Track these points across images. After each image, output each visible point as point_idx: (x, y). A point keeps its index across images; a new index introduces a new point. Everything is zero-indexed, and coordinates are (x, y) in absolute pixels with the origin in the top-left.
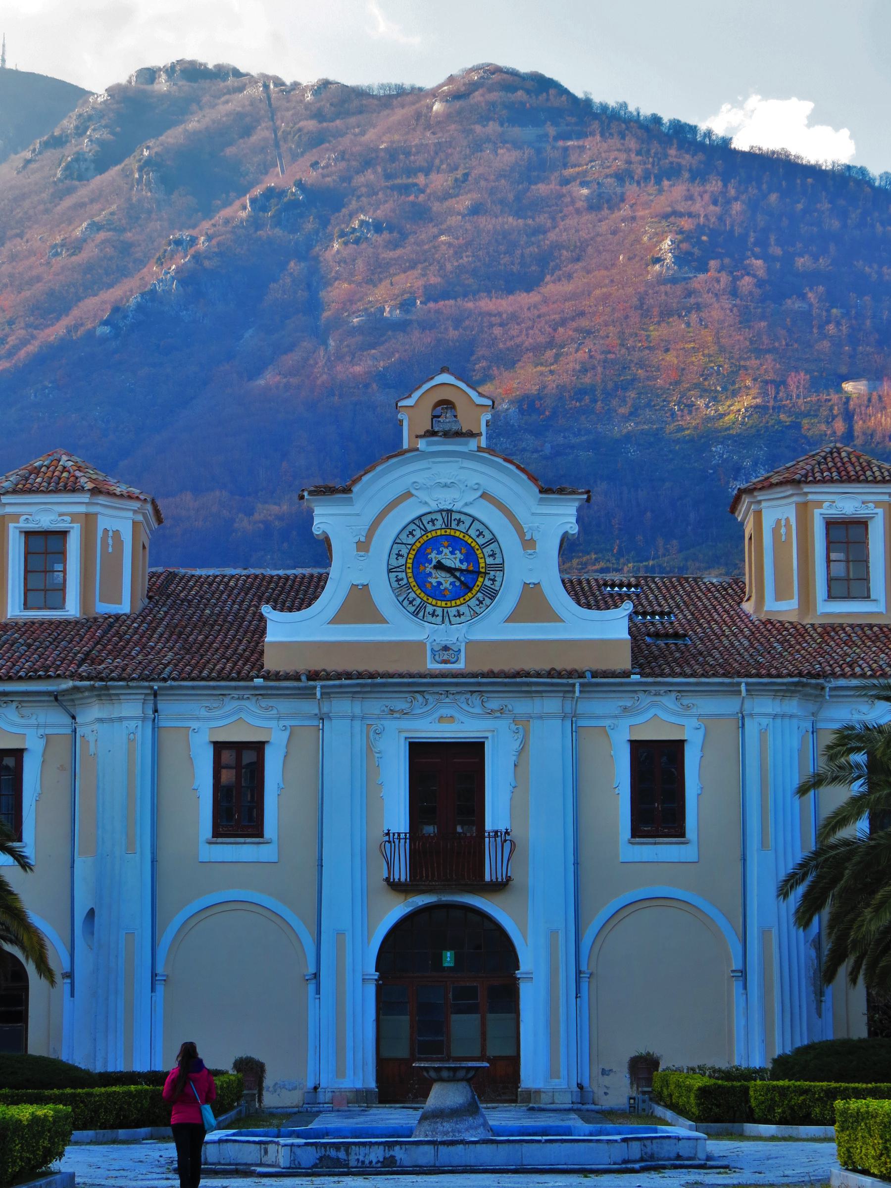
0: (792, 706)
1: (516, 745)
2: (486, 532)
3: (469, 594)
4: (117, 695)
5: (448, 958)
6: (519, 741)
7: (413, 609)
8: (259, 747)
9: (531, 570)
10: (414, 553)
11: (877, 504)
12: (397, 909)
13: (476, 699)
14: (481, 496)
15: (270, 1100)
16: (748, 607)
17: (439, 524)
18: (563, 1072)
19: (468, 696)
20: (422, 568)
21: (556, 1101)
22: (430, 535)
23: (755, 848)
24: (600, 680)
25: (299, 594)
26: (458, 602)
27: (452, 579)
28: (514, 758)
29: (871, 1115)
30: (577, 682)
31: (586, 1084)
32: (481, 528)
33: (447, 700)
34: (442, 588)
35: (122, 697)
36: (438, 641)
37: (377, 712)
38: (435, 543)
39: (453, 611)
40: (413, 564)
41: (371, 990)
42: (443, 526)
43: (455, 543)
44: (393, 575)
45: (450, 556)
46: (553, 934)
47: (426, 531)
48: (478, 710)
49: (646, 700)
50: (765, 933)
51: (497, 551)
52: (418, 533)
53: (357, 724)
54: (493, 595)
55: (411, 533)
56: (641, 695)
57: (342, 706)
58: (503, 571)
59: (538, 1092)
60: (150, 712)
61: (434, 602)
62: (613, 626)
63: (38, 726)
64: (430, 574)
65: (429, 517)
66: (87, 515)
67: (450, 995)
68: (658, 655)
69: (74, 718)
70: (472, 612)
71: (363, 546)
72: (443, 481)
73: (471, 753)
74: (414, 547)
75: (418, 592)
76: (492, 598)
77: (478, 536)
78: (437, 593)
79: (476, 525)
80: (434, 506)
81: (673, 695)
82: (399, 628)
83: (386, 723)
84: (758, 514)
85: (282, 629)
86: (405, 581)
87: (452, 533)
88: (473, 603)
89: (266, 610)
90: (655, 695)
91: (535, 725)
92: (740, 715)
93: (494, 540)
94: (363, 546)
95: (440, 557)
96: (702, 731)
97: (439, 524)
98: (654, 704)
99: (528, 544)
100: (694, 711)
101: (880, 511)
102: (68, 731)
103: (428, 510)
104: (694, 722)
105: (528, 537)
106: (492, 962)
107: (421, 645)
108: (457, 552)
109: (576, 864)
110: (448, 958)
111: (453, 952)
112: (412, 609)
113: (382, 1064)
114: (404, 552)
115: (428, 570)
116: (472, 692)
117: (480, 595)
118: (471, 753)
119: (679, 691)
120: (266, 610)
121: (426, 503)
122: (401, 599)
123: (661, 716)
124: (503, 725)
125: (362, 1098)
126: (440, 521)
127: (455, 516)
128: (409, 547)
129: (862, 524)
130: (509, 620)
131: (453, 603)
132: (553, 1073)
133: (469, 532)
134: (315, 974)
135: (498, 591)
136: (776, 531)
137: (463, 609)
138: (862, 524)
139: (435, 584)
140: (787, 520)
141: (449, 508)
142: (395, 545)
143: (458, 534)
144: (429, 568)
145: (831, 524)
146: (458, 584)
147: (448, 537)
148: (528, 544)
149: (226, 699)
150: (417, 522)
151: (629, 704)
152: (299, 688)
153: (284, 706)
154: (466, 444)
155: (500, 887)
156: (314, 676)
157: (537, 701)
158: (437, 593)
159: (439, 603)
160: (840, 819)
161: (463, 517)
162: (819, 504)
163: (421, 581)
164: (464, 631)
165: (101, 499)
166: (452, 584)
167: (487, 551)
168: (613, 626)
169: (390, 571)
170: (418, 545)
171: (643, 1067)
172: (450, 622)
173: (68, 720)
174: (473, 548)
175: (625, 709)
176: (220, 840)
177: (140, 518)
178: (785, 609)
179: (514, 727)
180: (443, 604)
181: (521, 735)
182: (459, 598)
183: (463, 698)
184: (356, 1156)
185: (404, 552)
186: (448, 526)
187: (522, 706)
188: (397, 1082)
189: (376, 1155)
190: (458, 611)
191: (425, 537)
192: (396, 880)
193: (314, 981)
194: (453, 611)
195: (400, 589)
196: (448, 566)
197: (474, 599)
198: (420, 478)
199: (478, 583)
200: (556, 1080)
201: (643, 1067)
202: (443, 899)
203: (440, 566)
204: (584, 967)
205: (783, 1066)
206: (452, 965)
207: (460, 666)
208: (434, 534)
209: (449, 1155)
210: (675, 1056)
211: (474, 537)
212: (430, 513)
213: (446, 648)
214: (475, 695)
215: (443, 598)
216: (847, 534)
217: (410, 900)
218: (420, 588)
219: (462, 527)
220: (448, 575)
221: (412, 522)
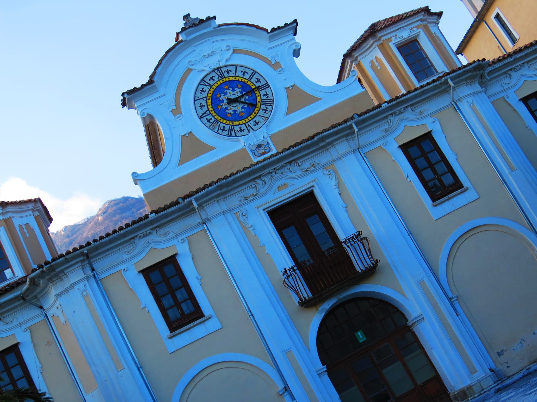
1: (334, 182)
2: (247, 70)
3: (256, 109)
4: (62, 271)
5: (360, 336)
6: (334, 179)
7: (227, 133)
8: (172, 260)
9: (285, 79)
10: (210, 101)
11: (417, 27)
12: (314, 319)
13: (294, 167)
14: (233, 53)
17: (216, 78)
18: (477, 367)
19: (289, 166)
20: (219, 107)
21: (484, 387)
23: (508, 173)
26: (252, 116)
27: (241, 106)
28: (337, 190)
30: (352, 122)
31: (493, 367)
32: (244, 69)
33: (277, 175)
34: (238, 113)
35: (66, 271)
36: (252, 144)
37: (237, 203)
38: (220, 89)
39: (252, 123)
40: (212, 107)
41: (326, 378)
42: (220, 78)
43: (232, 84)
44: (204, 119)
46: (421, 283)
47: (211, 86)
48: (299, 173)
49: (395, 120)
51: (260, 77)
52: (206, 89)
53: (229, 215)
55: (202, 91)
56: (391, 118)
57: (213, 209)
58: (269, 87)
59: (470, 388)
60: (90, 273)
61: (237, 123)
63: (20, 324)
64: (226, 109)
65: (208, 77)
66: (5, 221)
67: (375, 359)
69: (41, 307)
70: (264, 118)
71: (177, 111)
72: (206, 53)
74: (208, 98)
76: (272, 105)
77: (244, 75)
78: (236, 117)
80: (208, 70)
81: (409, 109)
82: (224, 149)
83: (246, 207)
84: (359, 66)
86: (213, 120)
87: (227, 79)
88: (261, 113)
90: (399, 114)
91: (338, 165)
92: (453, 103)
93: (254, 72)
94: (177, 111)
95: (227, 96)
96: (437, 122)
97: (216, 78)
98: (402, 120)
100: (426, 113)
101: (420, 30)
102: (42, 318)
103: (205, 73)
104: (430, 120)
105: (273, 62)
107: (243, 150)
108: (236, 89)
109: (410, 234)
110: (360, 336)
111: (361, 331)
114: (204, 103)
115: (224, 107)
116: (290, 163)
117: (263, 107)
119: (411, 105)
121: (202, 70)
122: (216, 130)
126: (217, 76)
127: (223, 70)
128: (205, 99)
130: (288, 113)
131: (249, 118)
132: (472, 371)
133: (237, 75)
134: (285, 388)
135: (273, 100)
136: (373, 67)
137: (257, 119)
139: (232, 113)
140: (376, 58)
141: (218, 66)
142: (196, 102)
143: (231, 79)
147: (225, 83)
148: (276, 66)
149: (136, 241)
150: (202, 83)
151: (386, 127)
152: (179, 210)
153: (175, 228)
154: (209, 26)
155: (372, 271)
157: (332, 150)
158: (236, 117)
159: (241, 122)
161: (229, 68)
162: (390, 40)
163: (223, 115)
164: (265, 131)
165: (9, 208)
167: (254, 80)
169: (200, 118)
170: (210, 95)
172: (253, 130)
173: (39, 311)
174: (244, 82)
175: (386, 130)
176: (177, 332)
177: (37, 213)
179: (326, 172)
181: (333, 175)
182: (252, 114)
183: (286, 169)
185: (204, 103)
186: (223, 77)
187: (324, 158)
190: (255, 122)
191: (212, 89)
192: (307, 298)
193: (287, 393)
194: (252, 123)
195: (212, 125)
197: (261, 110)
198: (192, 58)
199: (258, 100)
200: (477, 374)
202: (341, 297)
203: (231, 101)
204: (450, 295)
206: (365, 339)
207: (274, 151)
208: (216, 85)
211: (242, 76)
212: (208, 74)
213: (259, 146)
214: (292, 164)
215: (241, 118)
217: (320, 308)
218: (224, 119)
219: (231, 74)
220: (238, 104)
221: (200, 84)
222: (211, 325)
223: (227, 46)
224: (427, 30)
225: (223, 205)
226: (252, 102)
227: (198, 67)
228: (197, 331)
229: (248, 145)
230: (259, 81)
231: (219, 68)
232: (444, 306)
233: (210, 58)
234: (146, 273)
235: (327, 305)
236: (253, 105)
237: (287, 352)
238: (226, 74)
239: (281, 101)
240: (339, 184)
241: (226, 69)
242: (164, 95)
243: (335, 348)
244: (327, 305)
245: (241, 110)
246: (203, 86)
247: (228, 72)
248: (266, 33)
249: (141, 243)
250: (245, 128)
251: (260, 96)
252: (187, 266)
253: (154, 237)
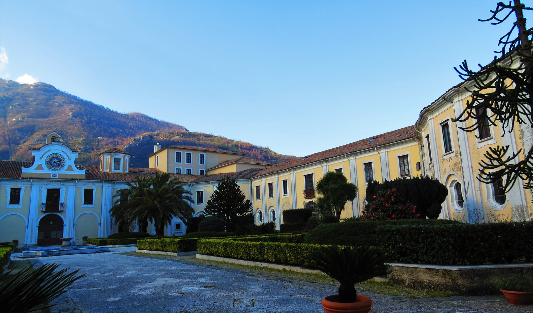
0: (110, 185)
5: (51, 223)
8: (20, 190)
12: (43, 215)
15: (19, 246)
16: (101, 170)
24: (80, 180)
25: (29, 165)
29: (147, 242)
38: (53, 158)
43: (57, 158)
49: (87, 183)
50: (104, 218)
54: (63, 167)
57: (35, 183)
62: (83, 172)
68: (90, 177)
71: (41, 158)
73: (58, 191)
78: (53, 166)
82: (46, 171)
85: (25, 170)
89: (22, 167)
94: (41, 158)
99: (70, 159)
106: (59, 224)
110: (51, 223)
113: (38, 240)
118: (58, 191)
120: (22, 167)
123: (89, 186)
124: (64, 187)
125: (35, 246)
129: (120, 159)
130: (66, 170)
138: (120, 159)
145: (115, 159)
148: (70, 159)
153: (25, 183)
155: (61, 211)
156: (31, 178)
160: (118, 201)
168: (83, 172)
171: (85, 238)
178: (108, 171)
184: (54, 253)
187: (67, 184)
188: (41, 242)
189: (57, 253)
195: (47, 165)
196: (56, 162)
198: (52, 148)
201: (85, 238)
203: (55, 162)
205: (110, 237)
207: (57, 177)
209: (69, 252)
210: (90, 237)
216: (117, 161)
222: (20, 206)
224: (124, 158)
225: (38, 183)
228: (16, 206)
232: (72, 224)
234: (12, 189)
235: (47, 214)
236: (59, 165)
237: (32, 220)
239: (66, 167)
240: (67, 191)
243: (43, 223)
244: (47, 214)
249: (14, 182)
252: (22, 192)
253: (18, 182)
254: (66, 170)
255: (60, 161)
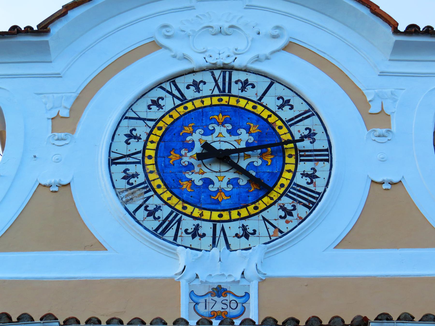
2: (295, 101)
3: (266, 199)
7: (157, 224)
9: (383, 160)
10: (160, 133)
14: (285, 48)
17: (206, 90)
20: (174, 156)
22: (190, 106)
26: (244, 213)
27: (232, 175)
34: (212, 188)
36: (203, 277)
38: (201, 117)
39: (232, 229)
40: (157, 150)
42: (216, 92)
43: (236, 117)
44: (118, 170)
45: (228, 137)
47: (184, 100)
51: (319, 129)
52: (168, 103)
54: (312, 200)
55: (155, 103)
58: (329, 160)
61: (197, 213)
64: (190, 167)
65: (189, 79)
70: (272, 229)
71: (64, 124)
72: (216, 24)
74: (160, 124)
75: (167, 195)
76: (311, 206)
77: (281, 107)
78: (204, 198)
79: (277, 90)
80: (199, 61)
87: (233, 101)
88: (274, 213)
93: (311, 112)
94: (64, 124)
95: (209, 139)
103: (185, 66)
105: (375, 108)
107: (171, 284)
108: (243, 131)
112: (153, 224)
114: (142, 130)
115: (186, 160)
117: (285, 200)
121: (185, 58)
122: (132, 207)
126: (211, 84)
127: (236, 76)
128: (151, 124)
130: (345, 243)
133: (264, 101)
135: (321, 195)
137: (251, 224)
139: (200, 183)
141: (228, 61)
142: (125, 122)
143: (242, 103)
144: (188, 157)
146: (243, 181)
147: (223, 108)
148: (377, 120)
150: (167, 86)
159: (207, 214)
161: (252, 78)
166: (233, 182)
167: (299, 130)
169: (112, 162)
170: (168, 120)
172: (228, 246)
174: (272, 126)
180: (215, 216)
182: (246, 206)
185: (142, 130)
190: (244, 228)
191: (181, 109)
194: (232, 229)
195: (131, 191)
197: (275, 208)
198: (176, 22)
199: (282, 181)
203: (209, 153)
208: (198, 104)
211: (275, 109)
212: (192, 72)
213: (220, 291)
215: (214, 205)
218: (168, 188)
219: (250, 93)
220: (224, 168)
221: (159, 85)
223: (278, 27)
226: (265, 178)
227: (177, 46)
229: (189, 274)
230: (311, 135)
231: (227, 69)
233: (221, 38)
236: (262, 186)
238: (235, 89)
241: (243, 76)
242: (58, 76)
245: (224, 185)
246: (162, 93)
247: (245, 84)
248: (389, 30)
250: (209, 233)
251: (294, 172)
254: (347, 242)
255: (269, 143)
